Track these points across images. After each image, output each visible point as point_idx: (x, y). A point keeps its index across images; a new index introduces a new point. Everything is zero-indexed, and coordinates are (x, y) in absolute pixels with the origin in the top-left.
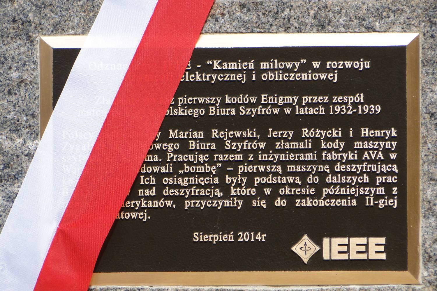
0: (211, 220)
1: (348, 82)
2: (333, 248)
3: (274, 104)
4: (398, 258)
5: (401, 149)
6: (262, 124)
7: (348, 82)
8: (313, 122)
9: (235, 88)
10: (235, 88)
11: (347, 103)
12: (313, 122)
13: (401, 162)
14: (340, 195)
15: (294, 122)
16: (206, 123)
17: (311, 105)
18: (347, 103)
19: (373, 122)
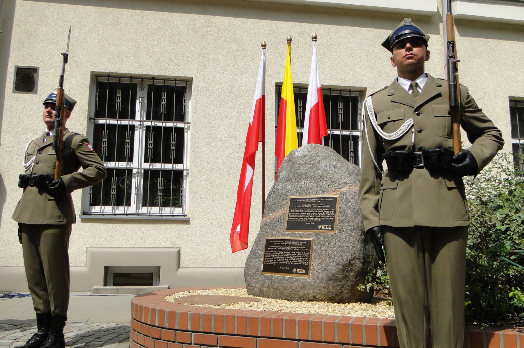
0: (283, 265)
1: (303, 245)
2: (298, 271)
3: (292, 248)
4: (307, 273)
5: (309, 256)
6: (291, 251)
7: (303, 245)
8: (298, 251)
9: (288, 245)
10: (288, 245)
11: (302, 248)
12: (298, 251)
13: (309, 258)
14: (300, 263)
15: (295, 251)
16: (283, 251)
17: (297, 249)
18: (302, 248)
19: (306, 251)
